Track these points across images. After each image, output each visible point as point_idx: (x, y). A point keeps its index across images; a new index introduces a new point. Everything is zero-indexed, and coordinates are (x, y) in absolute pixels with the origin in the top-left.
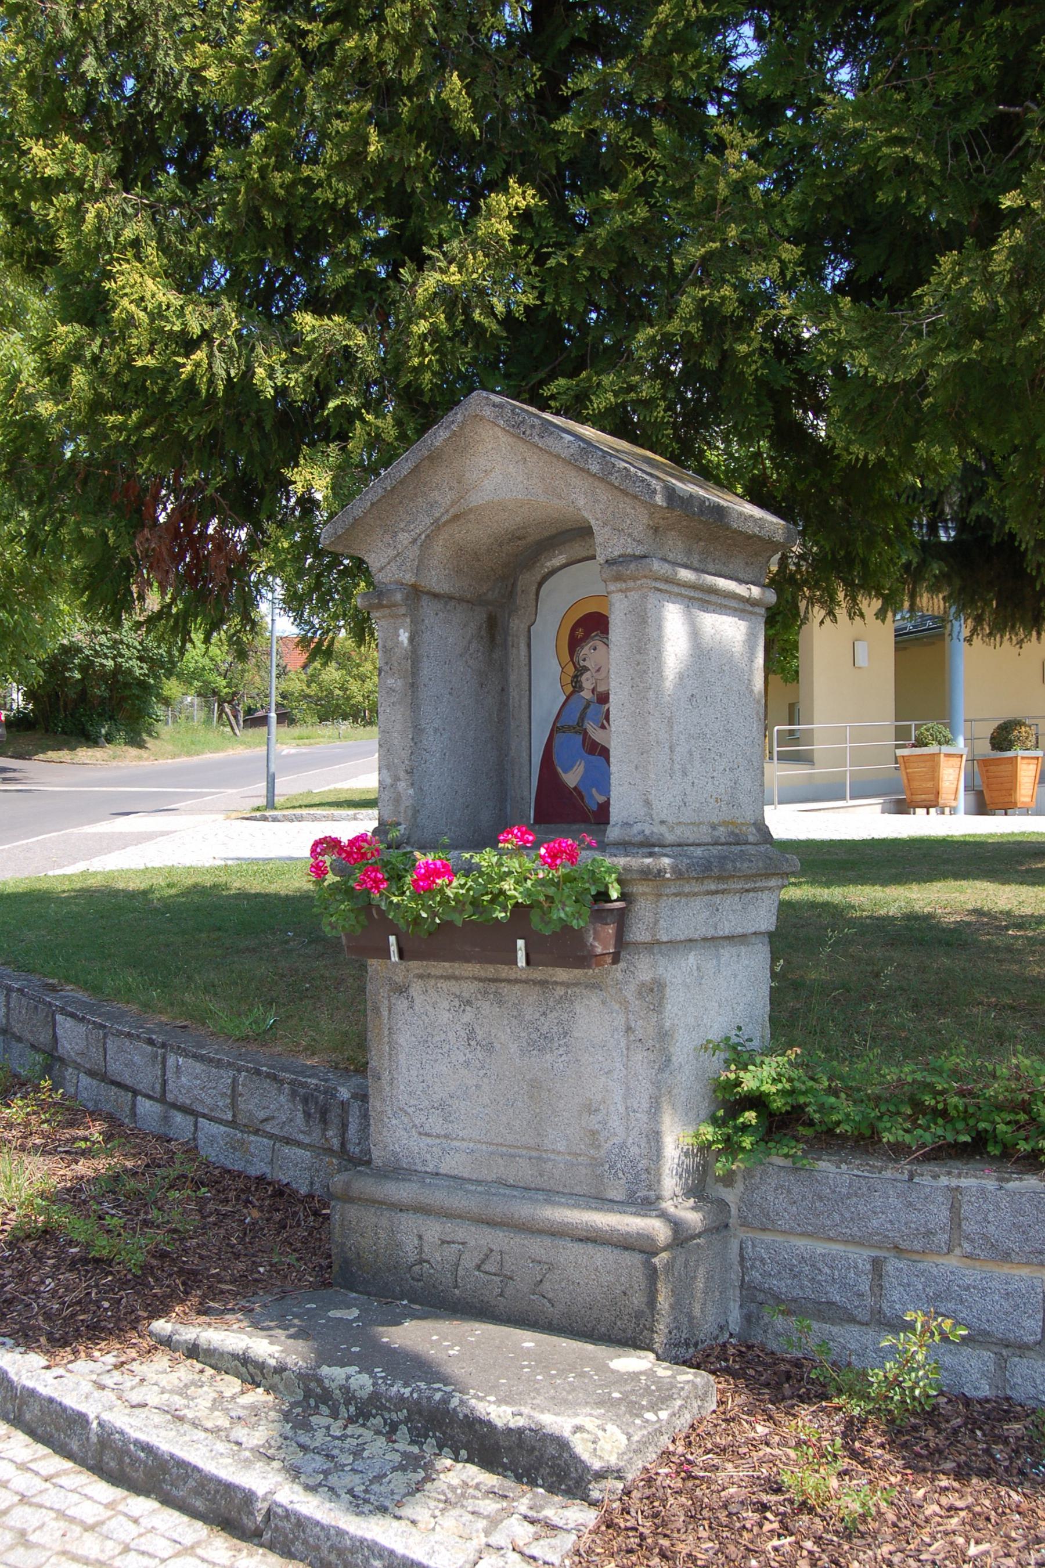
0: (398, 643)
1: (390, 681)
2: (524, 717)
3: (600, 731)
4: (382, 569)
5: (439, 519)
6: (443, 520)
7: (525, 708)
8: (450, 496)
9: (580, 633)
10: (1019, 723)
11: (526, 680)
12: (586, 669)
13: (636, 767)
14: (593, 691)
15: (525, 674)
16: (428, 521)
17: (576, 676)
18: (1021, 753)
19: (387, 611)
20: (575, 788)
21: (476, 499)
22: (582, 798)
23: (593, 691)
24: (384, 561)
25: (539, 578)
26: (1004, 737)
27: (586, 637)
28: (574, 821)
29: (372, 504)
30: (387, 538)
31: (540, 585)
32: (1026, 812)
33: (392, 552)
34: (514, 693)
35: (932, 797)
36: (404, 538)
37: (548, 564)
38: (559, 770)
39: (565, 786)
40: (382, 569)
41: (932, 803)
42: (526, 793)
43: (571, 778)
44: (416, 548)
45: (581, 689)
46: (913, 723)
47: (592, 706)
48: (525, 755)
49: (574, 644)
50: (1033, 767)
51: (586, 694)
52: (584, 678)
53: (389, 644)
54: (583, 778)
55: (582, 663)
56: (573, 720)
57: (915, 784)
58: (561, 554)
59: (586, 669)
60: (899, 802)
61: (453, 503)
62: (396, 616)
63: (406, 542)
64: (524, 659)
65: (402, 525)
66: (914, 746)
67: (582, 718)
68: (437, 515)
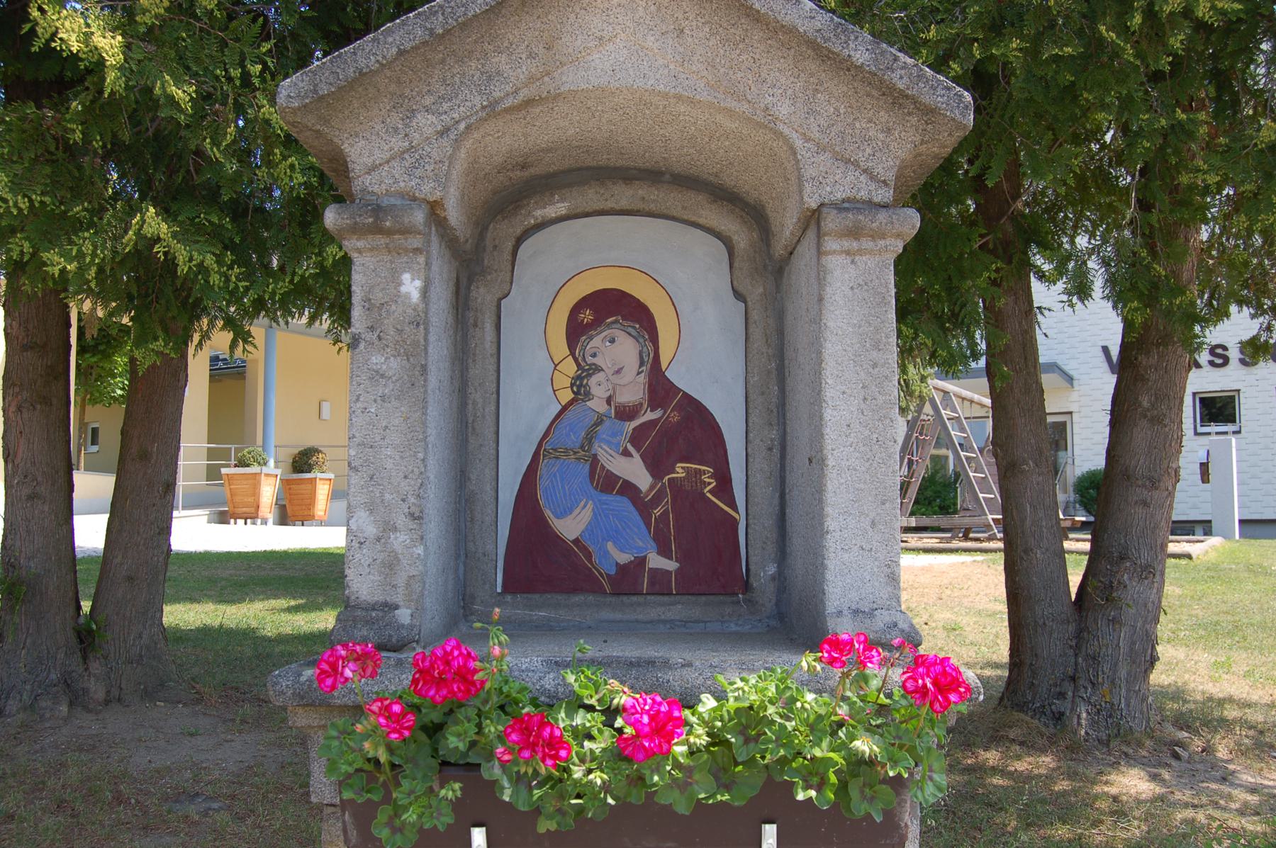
0: (397, 297)
1: (377, 360)
2: (489, 432)
3: (623, 459)
4: (372, 169)
5: (497, 102)
6: (509, 102)
7: (490, 420)
9: (587, 316)
10: (318, 451)
11: (494, 378)
12: (598, 369)
13: (873, 524)
15: (492, 368)
16: (478, 101)
17: (579, 377)
18: (320, 475)
19: (381, 240)
20: (576, 542)
21: (570, 79)
22: (589, 556)
24: (379, 156)
25: (519, 231)
26: (303, 462)
27: (597, 323)
28: (575, 590)
29: (401, 53)
30: (395, 119)
31: (519, 241)
32: (321, 523)
33: (398, 143)
34: (476, 396)
35: (253, 510)
36: (426, 123)
37: (538, 213)
38: (548, 513)
39: (557, 539)
40: (372, 169)
41: (251, 516)
42: (490, 547)
43: (570, 527)
44: (445, 142)
45: (588, 395)
46: (233, 447)
47: (607, 423)
48: (488, 488)
49: (576, 332)
50: (327, 487)
52: (593, 381)
53: (378, 296)
54: (590, 528)
55: (590, 360)
56: (575, 440)
57: (237, 499)
58: (562, 200)
59: (598, 369)
60: (222, 513)
61: (532, 79)
62: (399, 251)
63: (429, 131)
64: (489, 346)
65: (428, 100)
66: (236, 466)
67: (590, 438)
68: (497, 94)
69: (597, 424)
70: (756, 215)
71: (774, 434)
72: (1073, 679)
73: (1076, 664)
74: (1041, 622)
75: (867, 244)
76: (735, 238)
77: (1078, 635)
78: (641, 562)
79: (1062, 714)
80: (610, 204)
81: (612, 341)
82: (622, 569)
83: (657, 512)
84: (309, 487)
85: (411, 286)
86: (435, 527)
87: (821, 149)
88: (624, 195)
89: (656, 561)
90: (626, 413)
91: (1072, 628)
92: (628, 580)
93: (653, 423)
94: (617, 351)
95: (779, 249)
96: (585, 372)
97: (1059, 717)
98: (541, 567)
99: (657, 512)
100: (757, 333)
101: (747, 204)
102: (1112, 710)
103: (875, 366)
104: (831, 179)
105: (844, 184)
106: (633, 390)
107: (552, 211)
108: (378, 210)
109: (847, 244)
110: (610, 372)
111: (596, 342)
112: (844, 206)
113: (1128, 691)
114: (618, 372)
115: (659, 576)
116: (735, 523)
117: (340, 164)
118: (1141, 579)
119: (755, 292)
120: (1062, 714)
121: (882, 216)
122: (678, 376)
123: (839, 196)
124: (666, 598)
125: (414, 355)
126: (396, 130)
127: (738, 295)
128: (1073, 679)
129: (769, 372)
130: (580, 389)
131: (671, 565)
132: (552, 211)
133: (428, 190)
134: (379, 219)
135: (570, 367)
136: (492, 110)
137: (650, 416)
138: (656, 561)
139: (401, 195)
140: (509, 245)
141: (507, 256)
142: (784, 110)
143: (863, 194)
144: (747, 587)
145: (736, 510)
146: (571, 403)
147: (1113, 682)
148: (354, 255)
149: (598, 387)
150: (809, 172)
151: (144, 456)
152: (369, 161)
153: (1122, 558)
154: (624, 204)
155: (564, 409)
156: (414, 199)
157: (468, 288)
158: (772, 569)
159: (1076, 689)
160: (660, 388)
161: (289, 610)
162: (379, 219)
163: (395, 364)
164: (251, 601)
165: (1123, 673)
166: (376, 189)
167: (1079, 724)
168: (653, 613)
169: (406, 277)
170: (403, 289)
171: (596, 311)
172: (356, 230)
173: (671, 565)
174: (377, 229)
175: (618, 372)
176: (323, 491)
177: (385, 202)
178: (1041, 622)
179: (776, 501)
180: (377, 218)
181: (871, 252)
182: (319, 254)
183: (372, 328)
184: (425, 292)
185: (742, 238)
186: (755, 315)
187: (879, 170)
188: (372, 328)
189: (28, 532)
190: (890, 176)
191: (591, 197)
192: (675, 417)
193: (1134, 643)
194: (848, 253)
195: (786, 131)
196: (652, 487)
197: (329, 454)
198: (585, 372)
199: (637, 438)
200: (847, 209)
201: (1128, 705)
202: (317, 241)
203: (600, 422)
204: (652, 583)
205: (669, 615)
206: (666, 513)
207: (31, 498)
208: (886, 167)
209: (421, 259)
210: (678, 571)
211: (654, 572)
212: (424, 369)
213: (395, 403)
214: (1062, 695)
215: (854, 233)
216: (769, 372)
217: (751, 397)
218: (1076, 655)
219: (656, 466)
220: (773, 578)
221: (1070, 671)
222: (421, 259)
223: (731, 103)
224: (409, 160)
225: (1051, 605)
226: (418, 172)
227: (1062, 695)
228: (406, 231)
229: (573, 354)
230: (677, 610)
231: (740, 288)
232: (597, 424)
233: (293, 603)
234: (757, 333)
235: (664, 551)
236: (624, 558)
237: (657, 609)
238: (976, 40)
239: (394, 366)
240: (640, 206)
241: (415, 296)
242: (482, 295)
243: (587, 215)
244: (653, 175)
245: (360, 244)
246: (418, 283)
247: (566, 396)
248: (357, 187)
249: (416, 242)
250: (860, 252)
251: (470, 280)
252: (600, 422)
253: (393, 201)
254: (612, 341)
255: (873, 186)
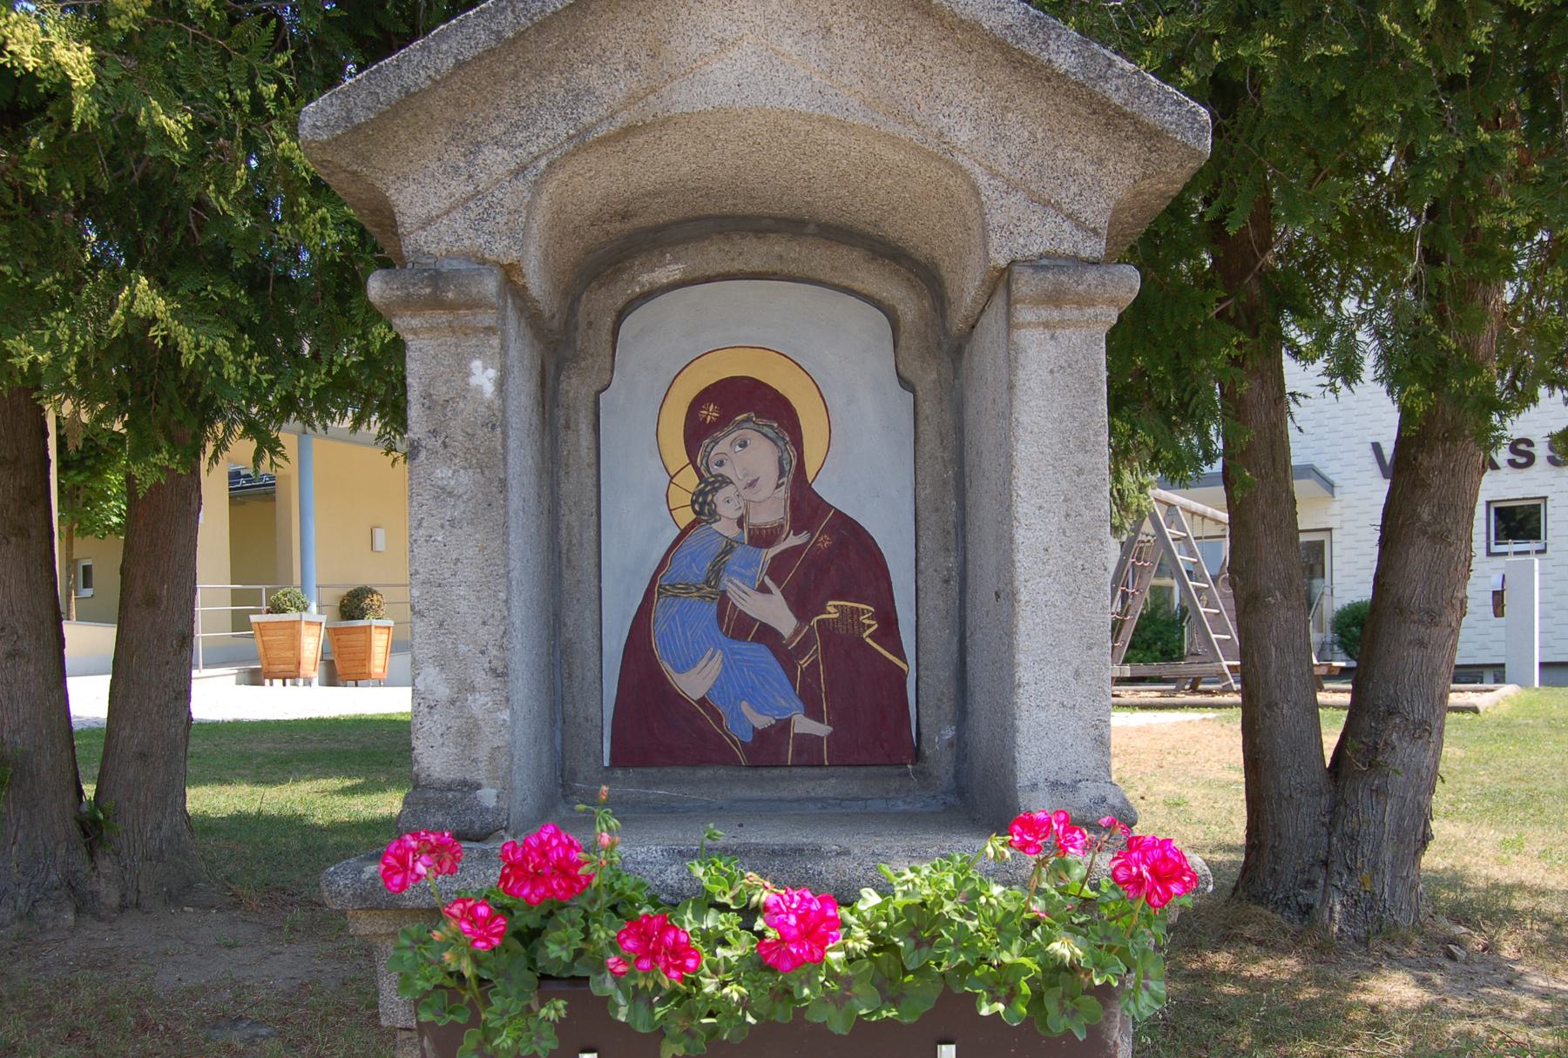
0: (465, 391)
1: (442, 473)
2: (588, 565)
3: (759, 597)
4: (428, 222)
5: (587, 130)
6: (602, 131)
7: (589, 548)
8: (625, 84)
9: (710, 413)
10: (372, 592)
11: (593, 495)
12: (725, 481)
14: (740, 522)
15: (590, 482)
16: (563, 129)
17: (701, 493)
18: (375, 622)
19: (443, 317)
22: (718, 719)
23: (740, 522)
24: (436, 205)
25: (620, 303)
26: (353, 605)
27: (724, 421)
28: (702, 762)
31: (621, 316)
32: (379, 683)
33: (459, 188)
34: (570, 518)
35: (292, 667)
36: (496, 160)
38: (666, 666)
39: (678, 699)
40: (428, 222)
41: (292, 674)
42: (593, 710)
43: (694, 683)
44: (520, 184)
45: (714, 515)
46: (264, 588)
47: (739, 551)
48: (590, 635)
49: (697, 434)
50: (385, 637)
51: (726, 527)
52: (720, 497)
53: (441, 391)
54: (718, 685)
55: (715, 470)
56: (697, 571)
57: (273, 654)
58: (676, 261)
59: (725, 481)
60: (254, 672)
62: (468, 331)
64: (586, 454)
66: (268, 612)
67: (717, 570)
69: (726, 552)
70: (927, 277)
71: (952, 562)
72: (1325, 863)
73: (1330, 844)
74: (1287, 794)
75: (1071, 313)
76: (901, 307)
77: (1333, 810)
78: (785, 725)
79: (1310, 907)
80: (737, 266)
81: (744, 445)
82: (761, 735)
83: (804, 663)
84: (362, 637)
85: (483, 377)
86: (523, 684)
87: (1012, 187)
88: (756, 253)
89: (803, 725)
90: (762, 538)
91: (1325, 801)
92: (768, 749)
93: (797, 550)
94: (750, 457)
95: (957, 322)
96: (709, 485)
97: (1306, 911)
98: (658, 734)
99: (804, 663)
100: (929, 432)
101: (916, 263)
102: (1373, 900)
103: (1080, 472)
104: (1024, 227)
105: (1044, 234)
106: (771, 508)
107: (663, 275)
108: (437, 277)
109: (1045, 313)
110: (741, 485)
111: (723, 446)
112: (1039, 264)
113: (1394, 877)
114: (752, 484)
115: (807, 743)
116: (901, 676)
117: (386, 216)
118: (1414, 738)
119: (927, 378)
120: (1310, 907)
121: (1091, 276)
122: (827, 488)
123: (1036, 249)
124: (816, 771)
125: (490, 465)
126: (456, 169)
127: (905, 383)
128: (1325, 863)
129: (945, 483)
130: (703, 507)
131: (822, 730)
132: (663, 275)
133: (500, 249)
134: (439, 289)
135: (690, 480)
136: (582, 142)
137: (793, 541)
138: (803, 725)
139: (467, 256)
140: (609, 321)
141: (606, 335)
142: (963, 135)
143: (1066, 247)
144: (917, 755)
145: (903, 659)
146: (692, 526)
147: (1375, 867)
148: (408, 337)
149: (727, 505)
150: (996, 219)
151: (152, 601)
152: (423, 212)
153: (1391, 713)
154: (756, 264)
155: (684, 533)
156: (484, 262)
157: (557, 379)
158: (949, 733)
159: (1328, 876)
160: (805, 505)
161: (344, 792)
162: (439, 289)
163: (465, 478)
164: (296, 781)
165: (1387, 855)
166: (433, 249)
167: (1331, 918)
168: (800, 790)
169: (477, 365)
170: (473, 381)
171: (721, 407)
172: (410, 304)
173: (822, 730)
174: (436, 303)
175: (752, 484)
176: (380, 642)
177: (446, 266)
178: (1287, 794)
179: (954, 647)
180: (436, 287)
181: (1076, 324)
182: (363, 336)
183: (434, 433)
184: (501, 384)
185: (910, 307)
186: (926, 408)
187: (1087, 215)
188: (434, 433)
189: (11, 699)
190: (1102, 222)
191: (714, 256)
192: (826, 542)
193: (1403, 819)
194: (1046, 325)
195: (966, 164)
196: (797, 632)
197: (385, 596)
198: (709, 485)
199: (777, 569)
200: (1045, 268)
201: (1393, 895)
202: (359, 319)
203: (729, 549)
204: (797, 753)
205: (820, 792)
206: (814, 665)
207: (11, 655)
208: (1097, 212)
209: (495, 341)
210: (830, 736)
211: (801, 738)
212: (503, 484)
213: (468, 529)
214: (1310, 884)
215: (1055, 298)
216: (945, 483)
217: (923, 514)
218: (1330, 834)
219: (802, 605)
220: (951, 744)
221: (1322, 854)
222: (495, 341)
223: (894, 128)
224: (475, 210)
225: (1299, 773)
226: (487, 226)
227: (1310, 884)
228: (474, 305)
229: (693, 462)
230: (830, 785)
231: (907, 375)
232: (726, 552)
233: (348, 783)
234: (929, 432)
235: (813, 712)
236: (762, 721)
237: (805, 785)
238: (1217, 36)
239: (463, 480)
240: (777, 266)
241: (489, 389)
242: (575, 387)
243: (708, 280)
244: (793, 226)
245: (415, 322)
246: (492, 373)
247: (686, 516)
248: (408, 246)
249: (487, 318)
250: (1063, 324)
251: (559, 368)
252: (729, 549)
253: (455, 264)
254: (744, 445)
255: (1079, 236)
